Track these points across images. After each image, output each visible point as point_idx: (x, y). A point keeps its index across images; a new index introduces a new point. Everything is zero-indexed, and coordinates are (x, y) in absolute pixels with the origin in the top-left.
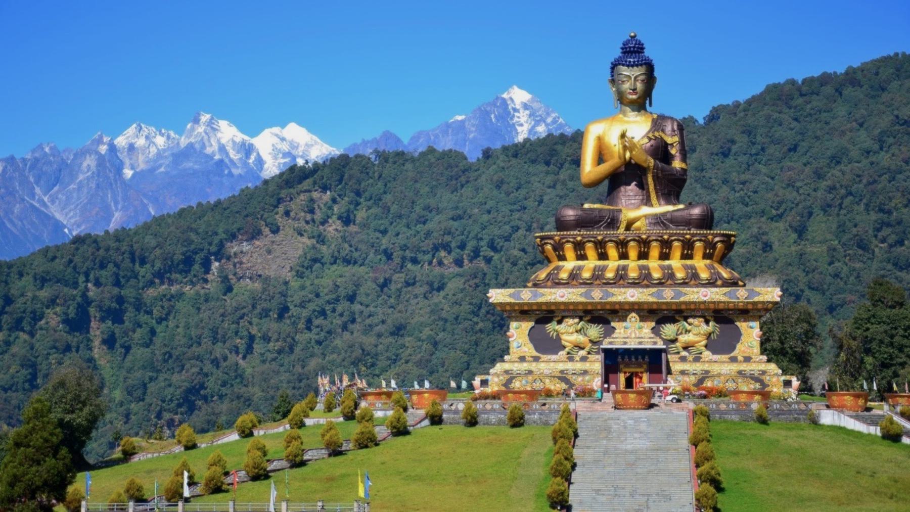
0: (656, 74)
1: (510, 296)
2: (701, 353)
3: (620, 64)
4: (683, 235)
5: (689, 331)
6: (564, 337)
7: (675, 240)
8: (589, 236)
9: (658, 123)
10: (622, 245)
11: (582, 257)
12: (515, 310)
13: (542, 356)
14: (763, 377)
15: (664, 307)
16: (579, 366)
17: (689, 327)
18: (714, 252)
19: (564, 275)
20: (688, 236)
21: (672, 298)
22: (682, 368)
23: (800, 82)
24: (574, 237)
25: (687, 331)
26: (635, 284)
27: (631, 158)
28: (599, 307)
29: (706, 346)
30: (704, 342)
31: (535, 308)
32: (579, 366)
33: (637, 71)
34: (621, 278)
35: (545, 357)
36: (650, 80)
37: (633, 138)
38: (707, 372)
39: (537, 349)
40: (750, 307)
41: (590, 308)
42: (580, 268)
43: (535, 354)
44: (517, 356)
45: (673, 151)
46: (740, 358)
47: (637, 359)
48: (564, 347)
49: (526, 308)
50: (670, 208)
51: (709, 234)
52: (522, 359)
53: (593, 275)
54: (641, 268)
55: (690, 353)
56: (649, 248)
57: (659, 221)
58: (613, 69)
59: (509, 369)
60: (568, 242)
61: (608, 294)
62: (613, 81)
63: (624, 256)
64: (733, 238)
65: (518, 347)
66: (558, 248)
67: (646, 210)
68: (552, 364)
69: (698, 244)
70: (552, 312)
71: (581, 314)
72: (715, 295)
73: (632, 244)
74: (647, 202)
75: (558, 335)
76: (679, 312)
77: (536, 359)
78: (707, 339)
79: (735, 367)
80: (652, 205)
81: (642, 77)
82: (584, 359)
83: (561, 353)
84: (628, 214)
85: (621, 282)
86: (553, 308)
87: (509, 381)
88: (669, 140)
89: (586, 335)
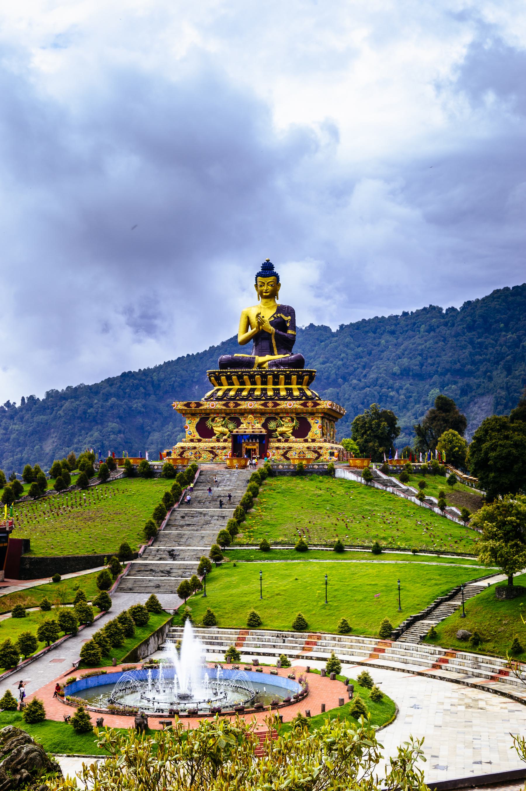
0: (280, 282)
1: (185, 405)
2: (289, 437)
3: (259, 276)
4: (285, 371)
5: (283, 425)
6: (214, 428)
7: (281, 374)
8: (234, 372)
10: (252, 377)
11: (232, 384)
12: (188, 413)
13: (202, 439)
14: (319, 450)
15: (268, 411)
16: (221, 444)
17: (283, 423)
18: (303, 381)
19: (220, 393)
20: (288, 372)
21: (272, 407)
22: (277, 446)
23: (511, 289)
24: (226, 372)
25: (282, 426)
26: (257, 399)
27: (262, 329)
28: (233, 412)
29: (293, 434)
30: (291, 431)
31: (198, 412)
32: (221, 444)
34: (250, 397)
35: (204, 440)
36: (277, 284)
37: (263, 317)
38: (291, 448)
39: (200, 435)
40: (315, 411)
41: (228, 411)
42: (230, 390)
43: (199, 437)
44: (189, 439)
45: (288, 325)
46: (310, 440)
47: (252, 440)
48: (215, 434)
49: (193, 412)
50: (282, 356)
51: (300, 371)
52: (192, 441)
53: (236, 394)
54: (262, 390)
55: (283, 438)
56: (267, 378)
58: (256, 278)
59: (183, 446)
60: (223, 375)
61: (276, 405)
62: (256, 285)
64: (314, 373)
65: (190, 434)
66: (218, 379)
67: (268, 357)
68: (207, 443)
69: (293, 377)
70: (209, 414)
71: (223, 415)
72: (296, 405)
73: (257, 377)
74: (272, 354)
75: (212, 428)
76: (278, 414)
77: (199, 441)
78: (293, 429)
79: (306, 445)
80: (274, 355)
81: (272, 283)
82: (225, 441)
83: (213, 437)
84: (260, 359)
85: (250, 398)
86: (208, 411)
87: (182, 453)
88: (286, 318)
89: (227, 427)
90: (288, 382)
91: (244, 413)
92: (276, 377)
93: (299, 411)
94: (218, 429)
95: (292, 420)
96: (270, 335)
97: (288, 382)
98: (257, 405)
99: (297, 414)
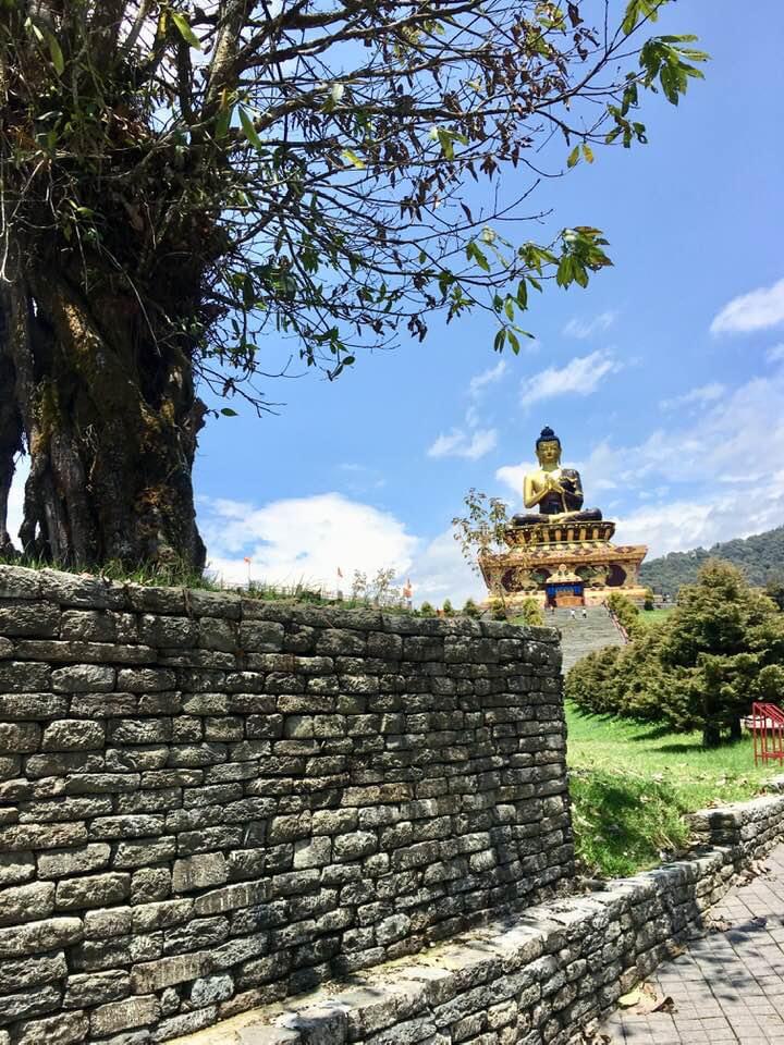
0: (562, 447)
9: (564, 472)
10: (552, 532)
15: (580, 560)
25: (595, 575)
33: (553, 444)
41: (536, 563)
50: (576, 513)
57: (570, 519)
63: (553, 539)
67: (561, 515)
70: (514, 567)
76: (589, 563)
88: (572, 480)
90: (589, 537)
91: (554, 565)
92: (577, 531)
93: (613, 558)
94: (526, 583)
95: (606, 569)
96: (560, 495)
97: (589, 537)
98: (568, 554)
99: (611, 561)
